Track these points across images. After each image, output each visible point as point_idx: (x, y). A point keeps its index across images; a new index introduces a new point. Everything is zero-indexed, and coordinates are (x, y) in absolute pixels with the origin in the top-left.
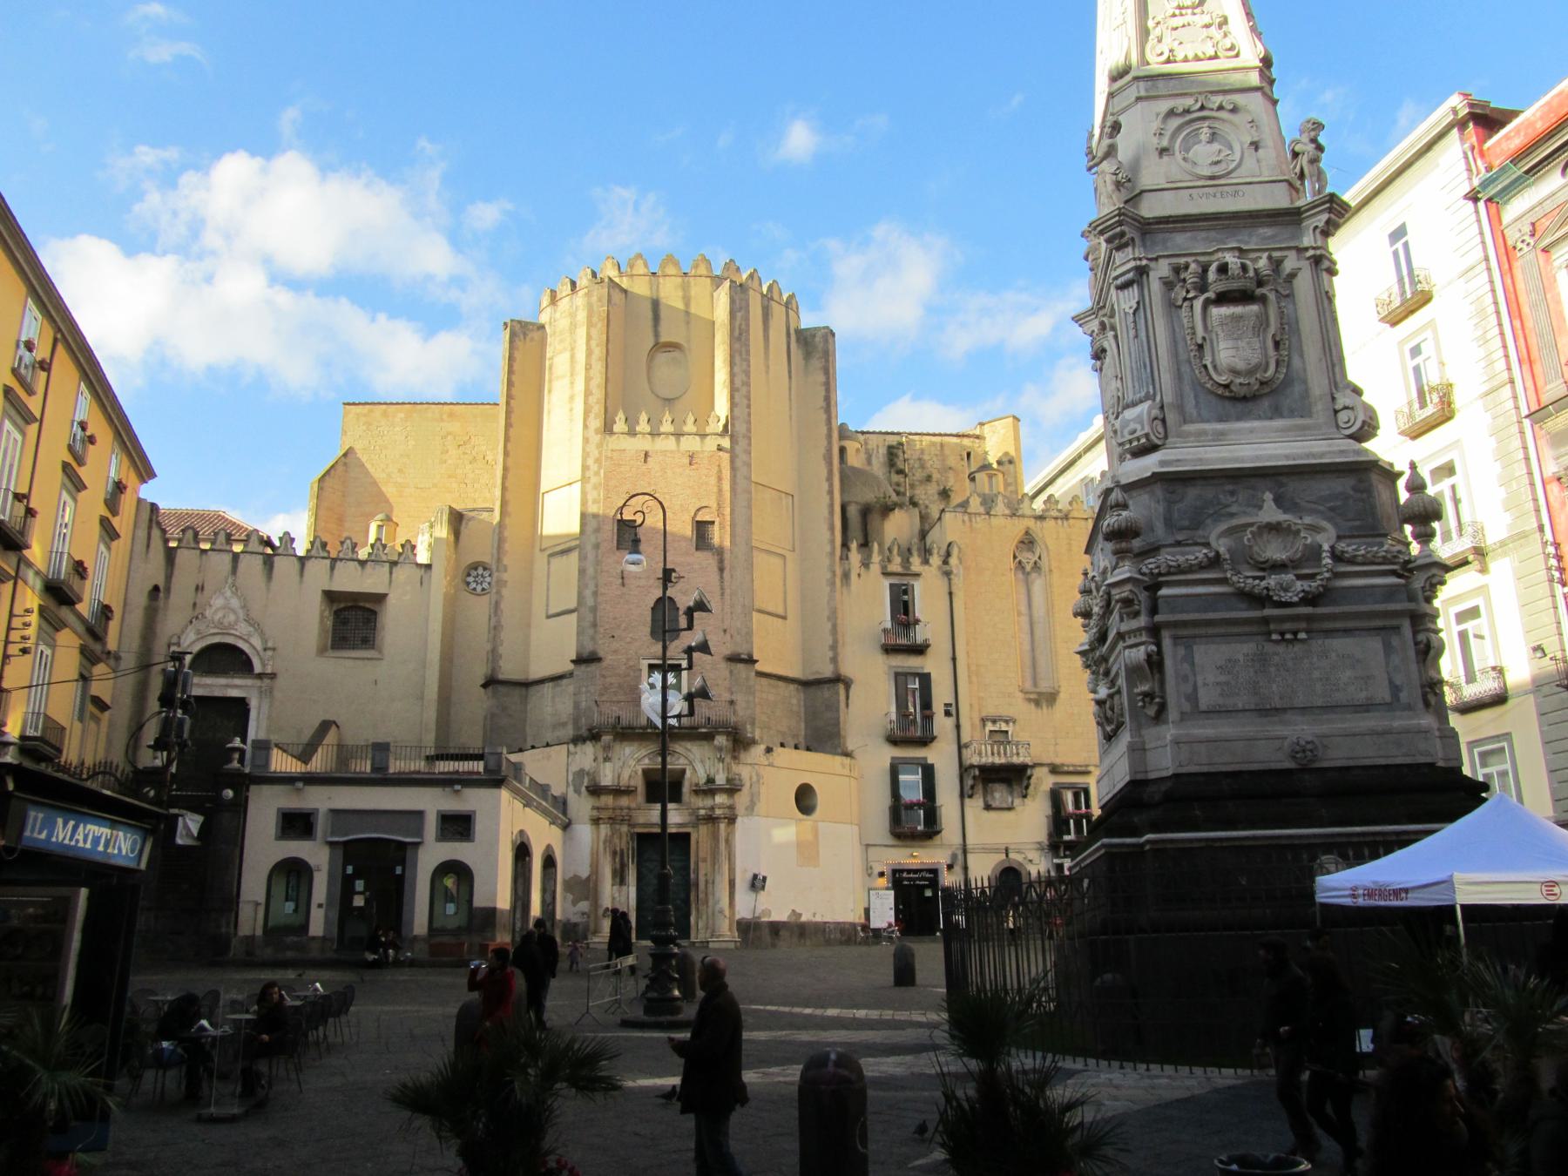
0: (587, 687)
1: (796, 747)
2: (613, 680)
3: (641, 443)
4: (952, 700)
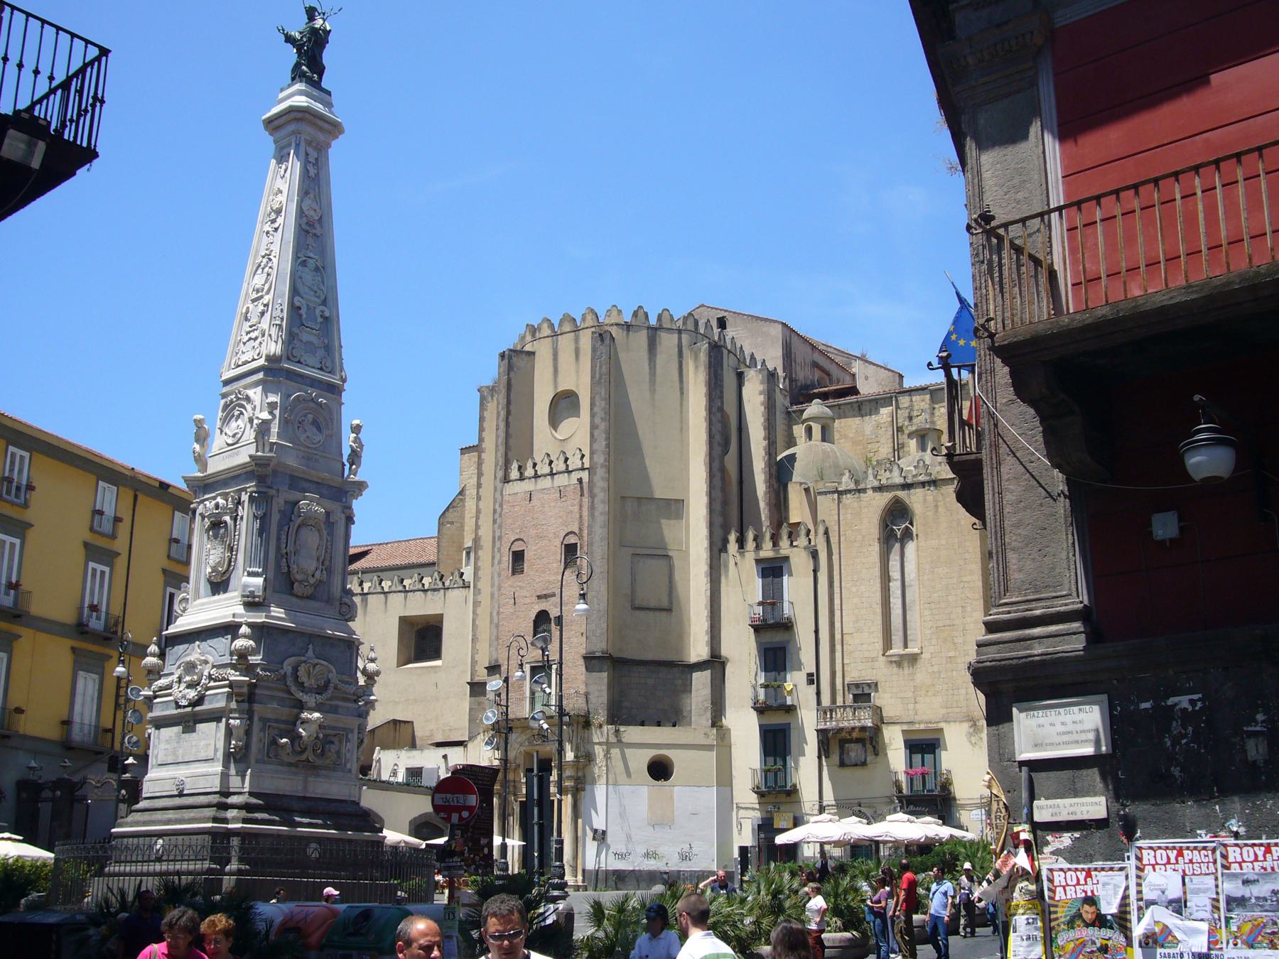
3: (527, 486)
4: (814, 671)
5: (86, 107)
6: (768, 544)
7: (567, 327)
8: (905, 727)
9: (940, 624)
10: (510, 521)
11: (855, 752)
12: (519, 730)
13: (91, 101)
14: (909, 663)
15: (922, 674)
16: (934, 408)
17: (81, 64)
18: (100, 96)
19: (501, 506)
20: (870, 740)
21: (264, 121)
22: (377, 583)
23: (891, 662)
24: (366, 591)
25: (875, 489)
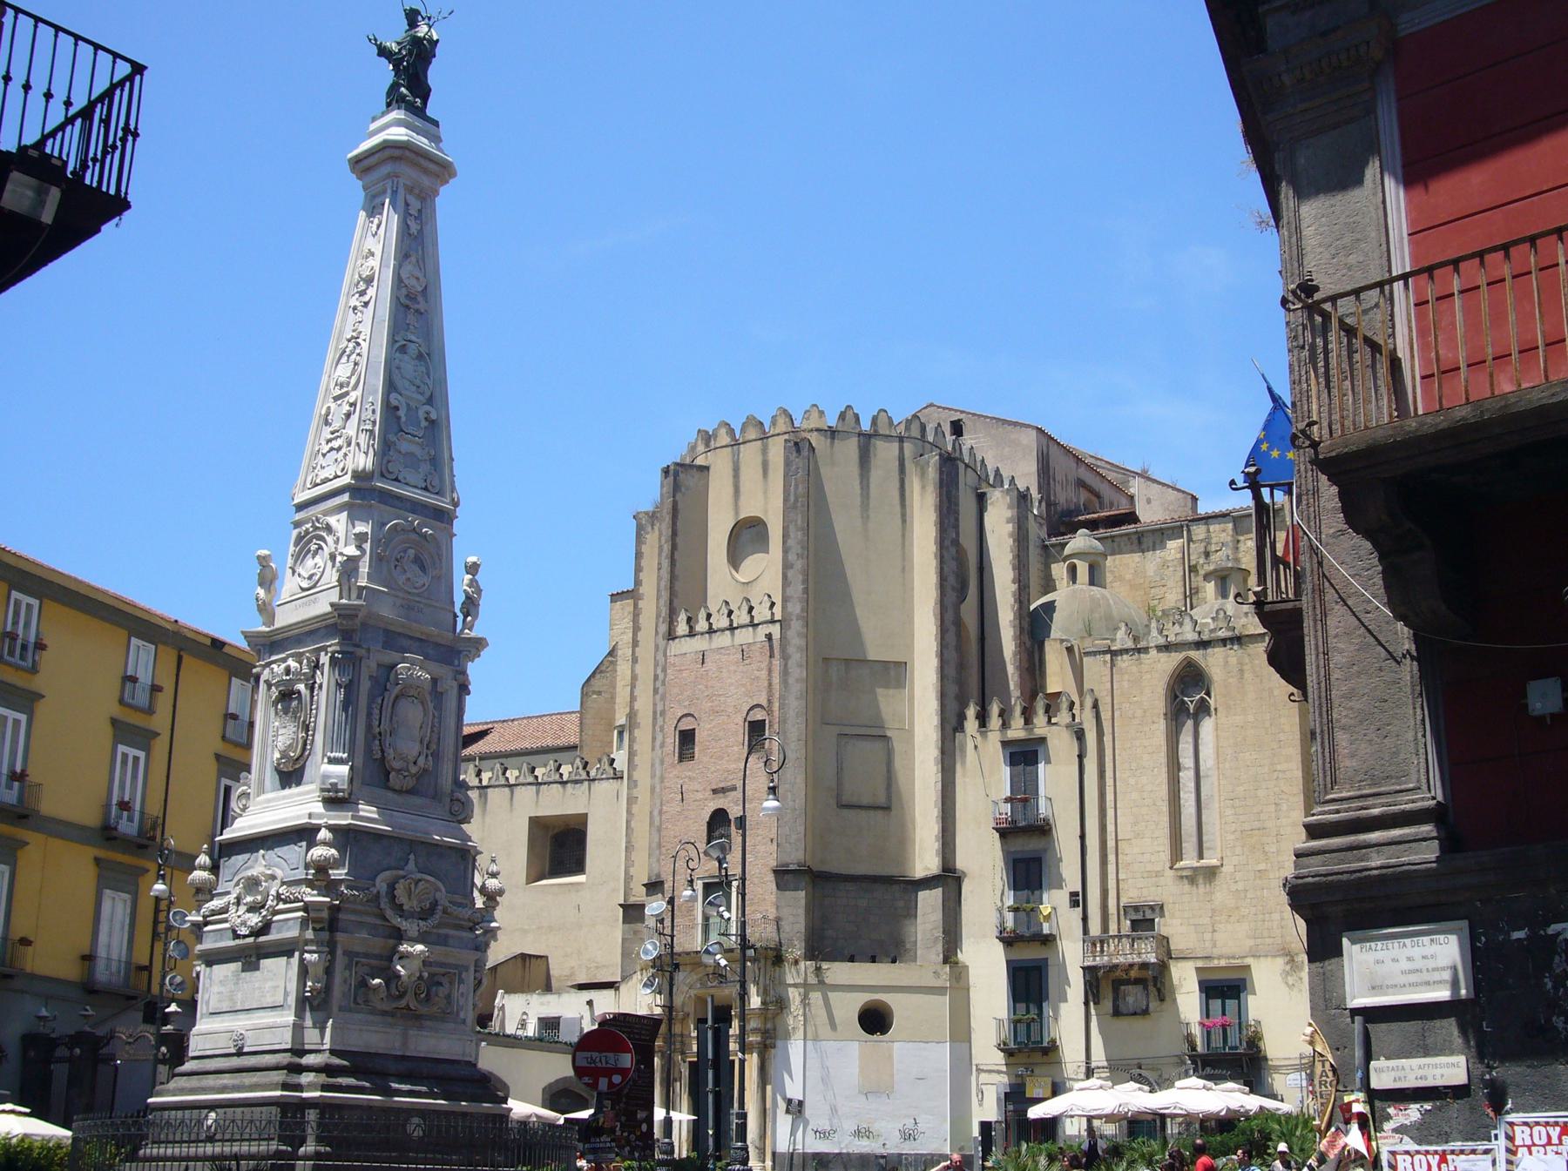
3: (699, 644)
4: (1079, 888)
5: (115, 141)
6: (1018, 721)
7: (752, 434)
8: (1200, 964)
9: (1247, 826)
10: (676, 690)
11: (1133, 996)
12: (689, 968)
13: (120, 134)
14: (1205, 878)
15: (1221, 893)
16: (1238, 541)
17: (107, 85)
18: (132, 127)
19: (664, 670)
20: (1154, 980)
21: (350, 160)
22: (500, 773)
23: (1182, 877)
24: (485, 783)
25: (1160, 648)
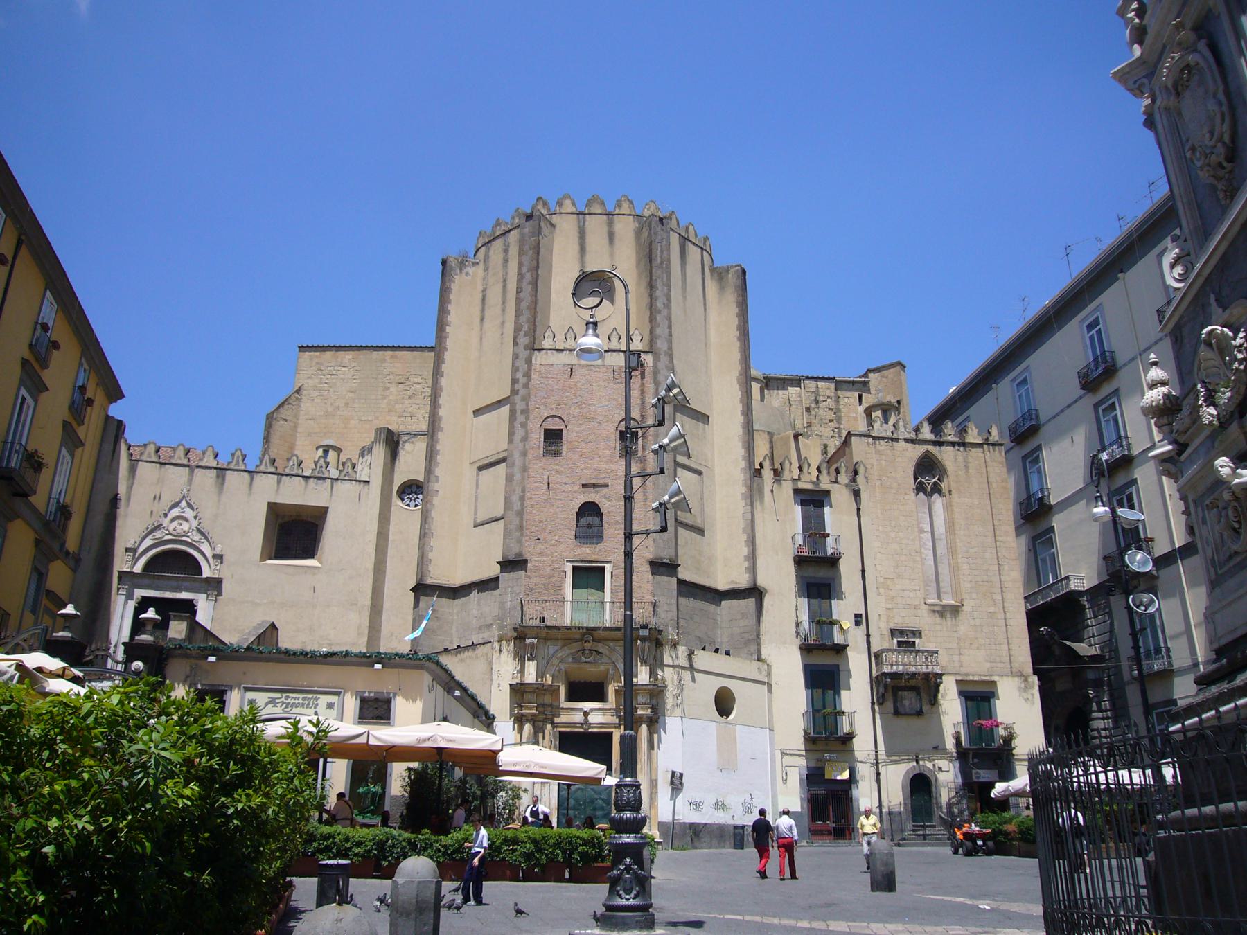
0: (512, 587)
1: (717, 651)
2: (537, 581)
8: (959, 678)
9: (979, 579)
11: (908, 700)
12: (560, 643)
14: (951, 614)
15: (964, 625)
16: (839, 397)
19: (528, 375)
20: (927, 686)
22: (240, 459)
23: (934, 611)
25: (907, 441)
